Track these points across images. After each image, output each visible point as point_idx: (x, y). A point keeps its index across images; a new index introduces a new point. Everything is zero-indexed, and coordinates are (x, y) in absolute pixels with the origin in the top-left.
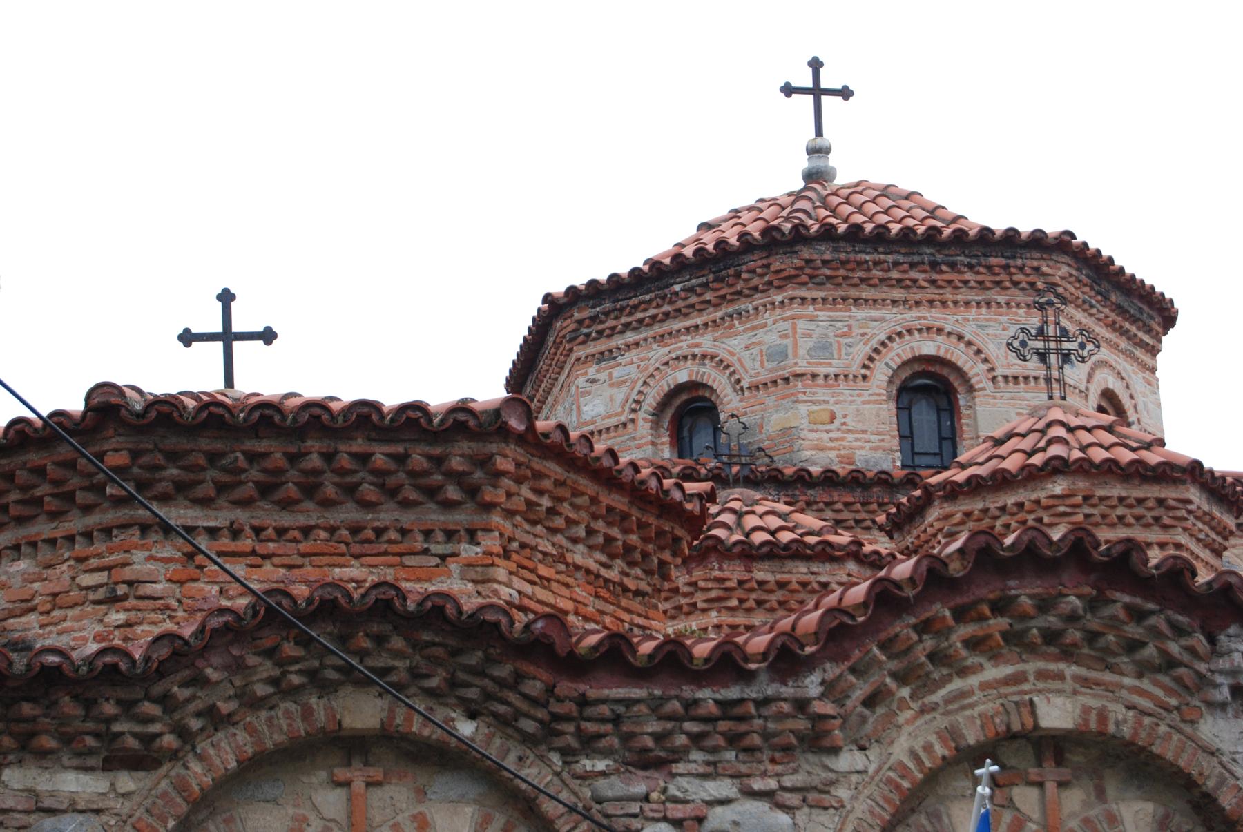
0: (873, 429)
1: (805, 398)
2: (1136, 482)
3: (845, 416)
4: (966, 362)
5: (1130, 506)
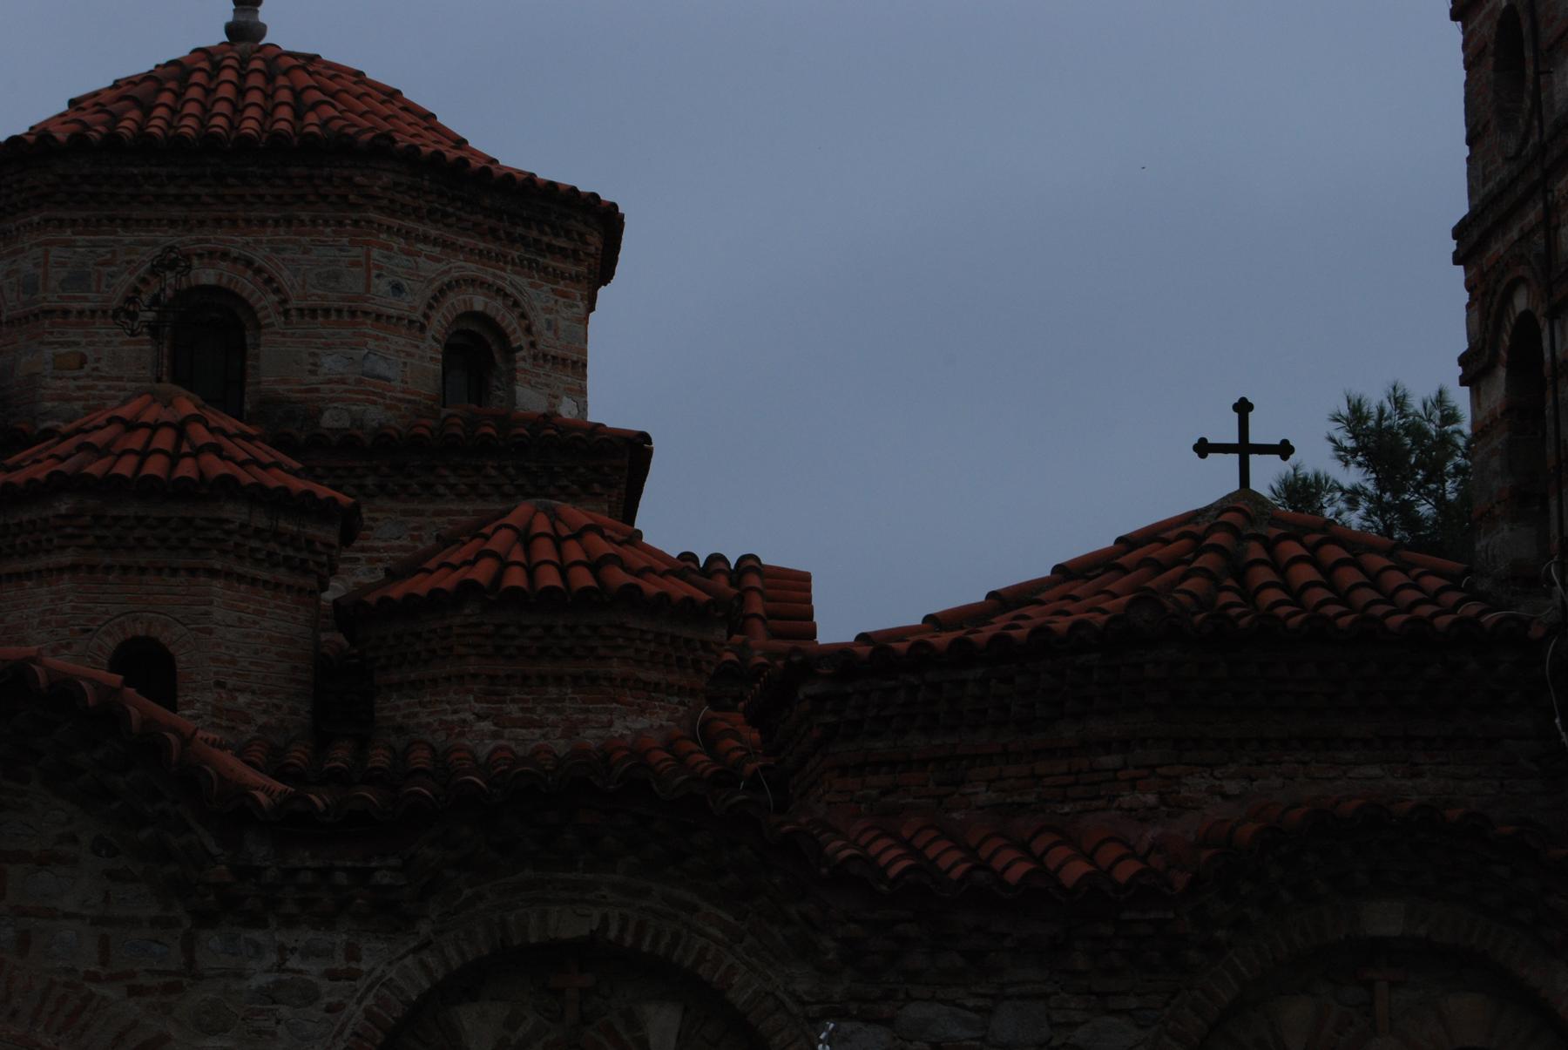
3: (98, 360)
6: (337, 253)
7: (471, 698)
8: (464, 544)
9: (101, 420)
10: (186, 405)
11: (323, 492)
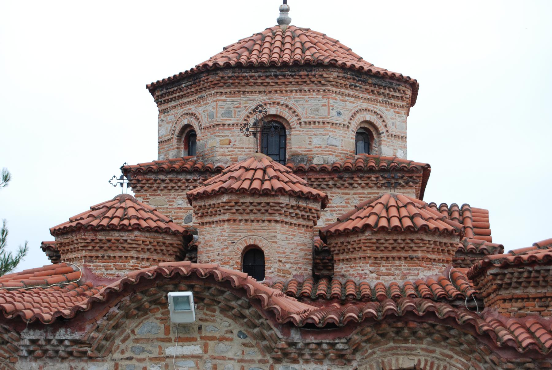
0: (247, 146)
1: (219, 134)
2: (257, 196)
3: (235, 141)
4: (289, 116)
5: (255, 206)
6: (318, 101)
7: (368, 265)
8: (365, 209)
9: (237, 168)
10: (266, 161)
11: (315, 192)
